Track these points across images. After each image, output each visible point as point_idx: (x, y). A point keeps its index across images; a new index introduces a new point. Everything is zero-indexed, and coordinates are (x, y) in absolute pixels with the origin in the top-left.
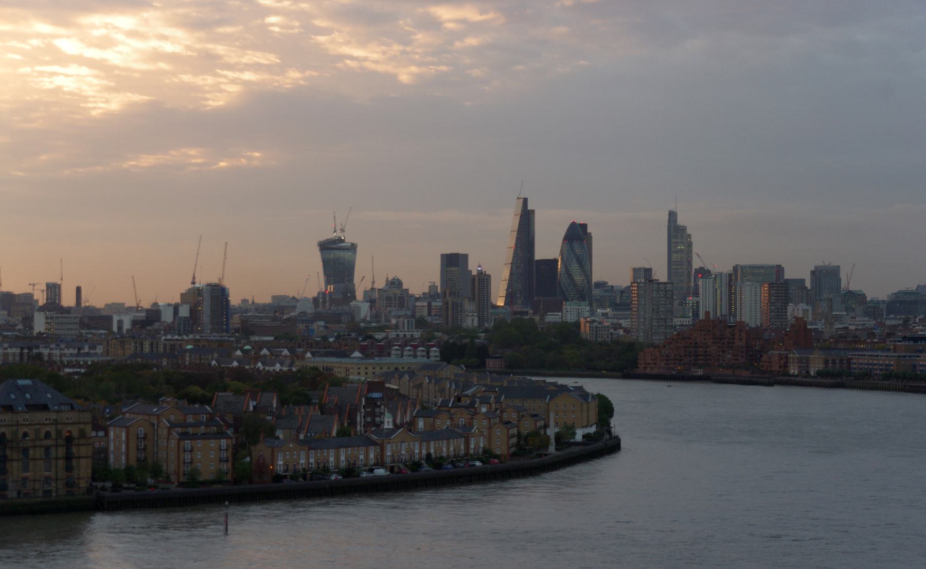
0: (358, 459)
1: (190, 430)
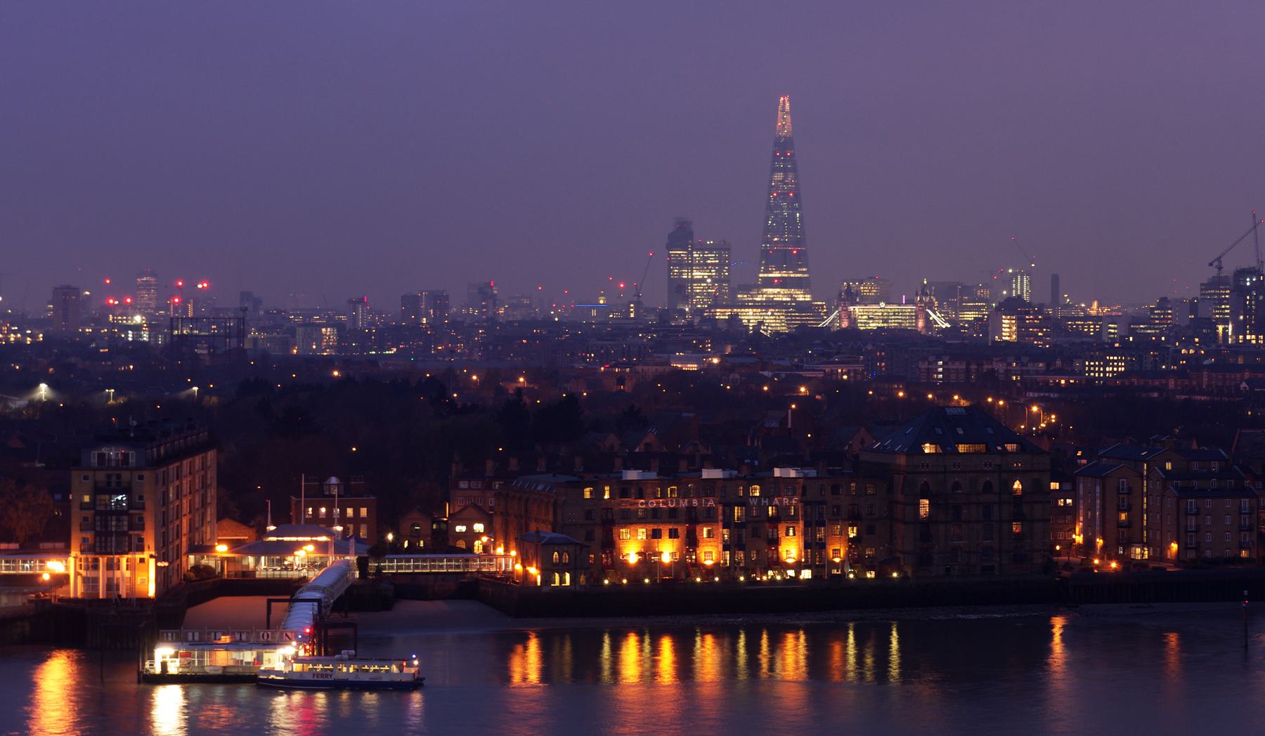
1: (1196, 483)
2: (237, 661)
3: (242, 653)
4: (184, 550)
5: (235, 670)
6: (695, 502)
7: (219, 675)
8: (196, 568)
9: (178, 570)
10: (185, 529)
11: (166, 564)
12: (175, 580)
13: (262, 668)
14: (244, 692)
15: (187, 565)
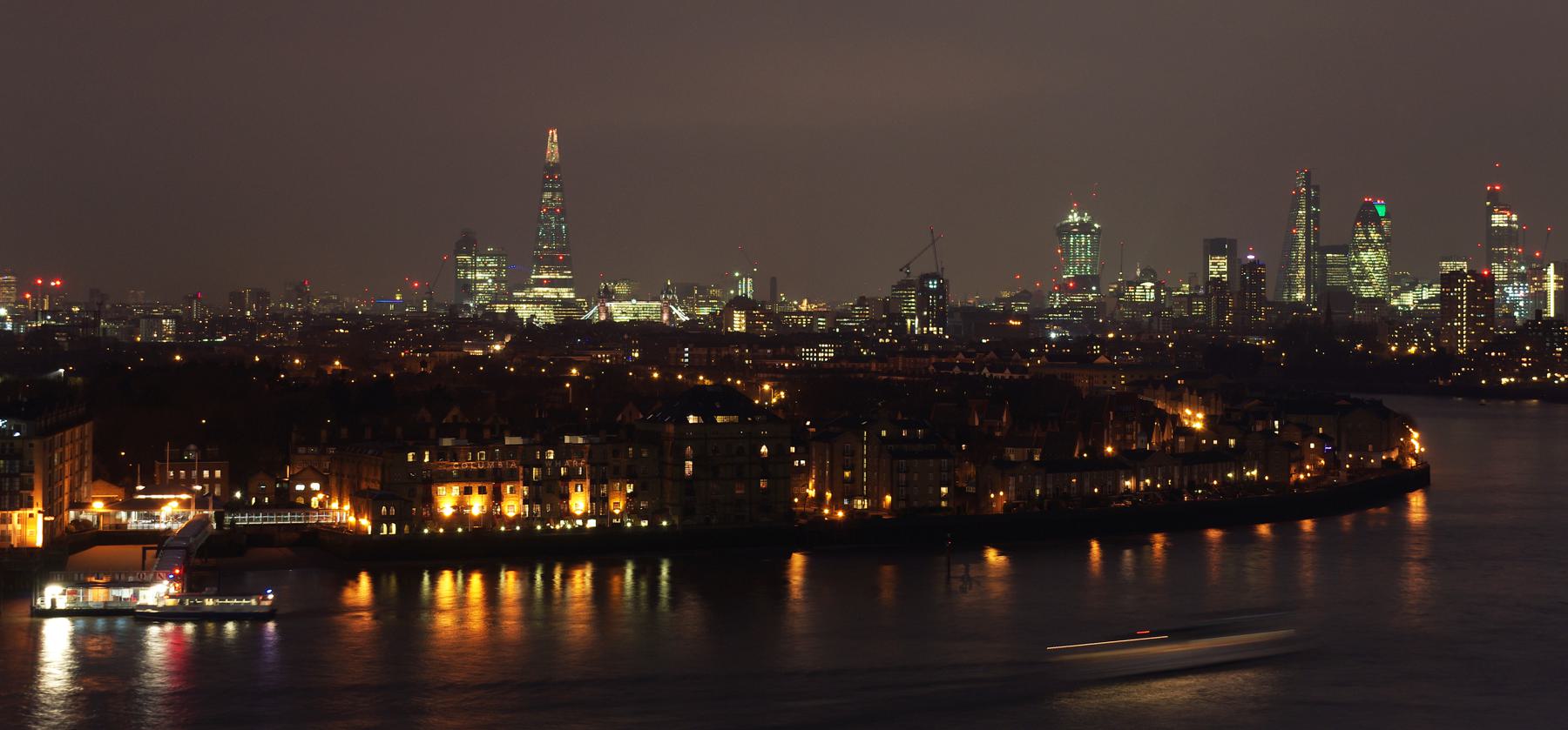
0: (1106, 485)
2: (115, 597)
3: (120, 591)
4: (66, 506)
5: (114, 605)
6: (500, 464)
7: (101, 609)
8: (76, 522)
9: (60, 524)
10: (66, 489)
11: (52, 518)
12: (58, 532)
13: (138, 603)
14: (121, 623)
15: (68, 519)
